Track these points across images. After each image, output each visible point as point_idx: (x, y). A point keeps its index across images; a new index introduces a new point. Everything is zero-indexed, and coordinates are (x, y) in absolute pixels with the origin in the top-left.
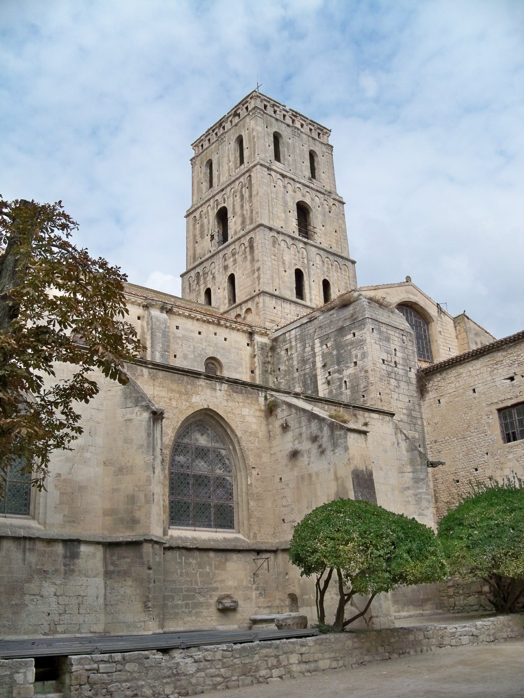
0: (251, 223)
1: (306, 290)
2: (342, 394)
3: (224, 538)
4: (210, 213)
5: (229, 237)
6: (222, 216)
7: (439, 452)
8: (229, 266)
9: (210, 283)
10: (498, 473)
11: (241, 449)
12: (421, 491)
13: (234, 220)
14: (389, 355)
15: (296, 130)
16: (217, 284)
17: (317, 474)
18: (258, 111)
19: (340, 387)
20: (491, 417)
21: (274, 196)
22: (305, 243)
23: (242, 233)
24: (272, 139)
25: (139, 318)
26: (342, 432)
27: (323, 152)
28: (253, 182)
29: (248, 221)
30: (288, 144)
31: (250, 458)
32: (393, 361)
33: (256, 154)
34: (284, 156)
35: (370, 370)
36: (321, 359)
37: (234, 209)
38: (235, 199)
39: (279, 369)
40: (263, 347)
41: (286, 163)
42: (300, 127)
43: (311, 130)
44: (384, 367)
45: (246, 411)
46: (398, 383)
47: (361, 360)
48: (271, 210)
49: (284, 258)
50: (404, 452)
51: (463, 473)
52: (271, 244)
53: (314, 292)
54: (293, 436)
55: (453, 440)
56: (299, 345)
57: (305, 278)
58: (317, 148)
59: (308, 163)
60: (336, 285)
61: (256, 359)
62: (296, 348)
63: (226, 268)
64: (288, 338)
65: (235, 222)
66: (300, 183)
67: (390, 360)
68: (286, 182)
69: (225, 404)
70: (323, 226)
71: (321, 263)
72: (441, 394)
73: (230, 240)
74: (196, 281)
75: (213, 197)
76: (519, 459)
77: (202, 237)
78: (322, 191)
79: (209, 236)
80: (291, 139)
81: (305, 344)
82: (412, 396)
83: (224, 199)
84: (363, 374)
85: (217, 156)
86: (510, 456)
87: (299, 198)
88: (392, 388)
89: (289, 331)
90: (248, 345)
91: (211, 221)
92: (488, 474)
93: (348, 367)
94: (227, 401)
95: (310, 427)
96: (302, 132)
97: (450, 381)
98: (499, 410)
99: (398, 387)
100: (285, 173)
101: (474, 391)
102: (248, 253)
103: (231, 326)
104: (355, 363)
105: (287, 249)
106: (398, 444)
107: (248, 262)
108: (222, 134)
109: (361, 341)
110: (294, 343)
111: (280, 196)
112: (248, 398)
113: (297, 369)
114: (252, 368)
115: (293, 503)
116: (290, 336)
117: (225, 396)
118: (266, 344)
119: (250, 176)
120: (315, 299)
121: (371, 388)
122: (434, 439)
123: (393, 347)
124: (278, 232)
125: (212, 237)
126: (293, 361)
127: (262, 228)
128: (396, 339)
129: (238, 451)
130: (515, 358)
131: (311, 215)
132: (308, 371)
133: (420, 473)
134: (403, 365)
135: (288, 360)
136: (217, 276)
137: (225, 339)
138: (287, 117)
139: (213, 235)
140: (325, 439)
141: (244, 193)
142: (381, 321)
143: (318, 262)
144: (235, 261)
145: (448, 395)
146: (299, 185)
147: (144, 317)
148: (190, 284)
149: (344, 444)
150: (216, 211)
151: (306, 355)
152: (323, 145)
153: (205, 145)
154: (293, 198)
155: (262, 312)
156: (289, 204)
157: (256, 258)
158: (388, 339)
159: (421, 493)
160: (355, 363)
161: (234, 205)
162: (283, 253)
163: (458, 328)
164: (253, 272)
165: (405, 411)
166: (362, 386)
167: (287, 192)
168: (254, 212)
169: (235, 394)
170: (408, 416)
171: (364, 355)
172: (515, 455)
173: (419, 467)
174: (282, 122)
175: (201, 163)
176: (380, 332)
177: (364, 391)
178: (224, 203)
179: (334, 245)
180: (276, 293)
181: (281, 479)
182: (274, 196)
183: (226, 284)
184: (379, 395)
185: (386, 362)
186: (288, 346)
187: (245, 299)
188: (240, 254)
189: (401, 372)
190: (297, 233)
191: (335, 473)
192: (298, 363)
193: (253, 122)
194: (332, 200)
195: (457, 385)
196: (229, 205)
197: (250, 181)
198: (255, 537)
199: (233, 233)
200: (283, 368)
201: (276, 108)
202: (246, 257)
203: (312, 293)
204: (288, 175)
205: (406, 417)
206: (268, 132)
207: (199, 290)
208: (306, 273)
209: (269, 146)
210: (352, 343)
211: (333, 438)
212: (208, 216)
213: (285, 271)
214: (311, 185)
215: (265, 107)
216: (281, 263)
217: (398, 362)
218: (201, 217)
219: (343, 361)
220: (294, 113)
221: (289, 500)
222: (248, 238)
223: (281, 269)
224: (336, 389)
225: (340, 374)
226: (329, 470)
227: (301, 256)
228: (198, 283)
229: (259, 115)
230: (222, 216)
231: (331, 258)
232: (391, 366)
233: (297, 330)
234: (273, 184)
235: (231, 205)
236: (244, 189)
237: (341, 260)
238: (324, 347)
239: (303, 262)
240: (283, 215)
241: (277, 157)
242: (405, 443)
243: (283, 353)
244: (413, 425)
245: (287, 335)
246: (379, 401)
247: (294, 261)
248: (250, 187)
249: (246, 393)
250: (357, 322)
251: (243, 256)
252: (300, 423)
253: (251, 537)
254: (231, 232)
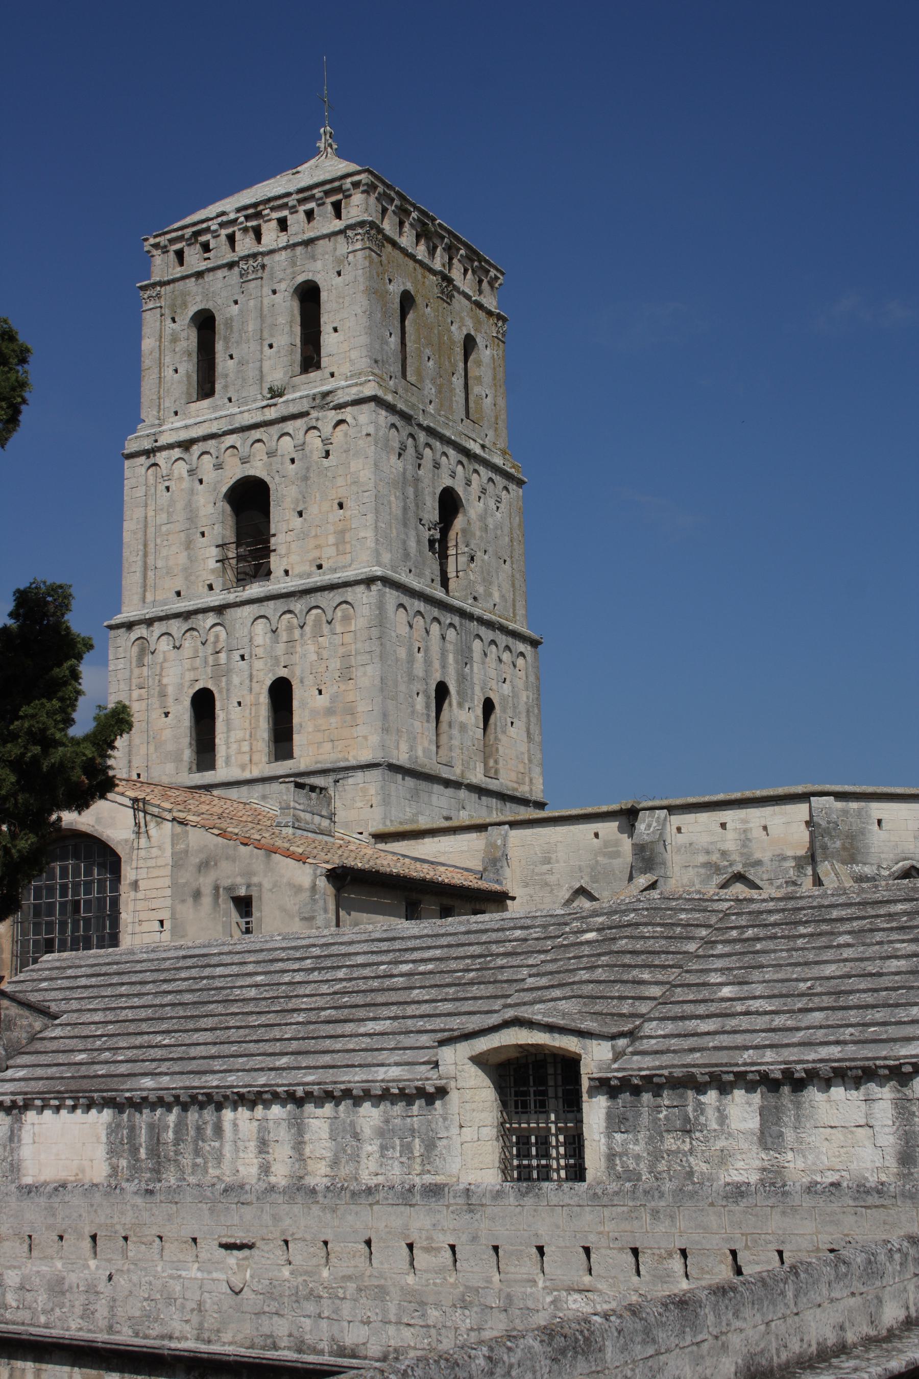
15: (251, 262)
21: (163, 517)
49: (165, 681)
58: (319, 265)
87: (234, 472)
111: (180, 505)
156: (202, 512)
162: (162, 669)
167: (201, 481)
179: (328, 555)
201: (203, 239)
208: (220, 692)
213: (167, 714)
216: (155, 702)
223: (157, 714)
231: (298, 606)
239: (217, 665)
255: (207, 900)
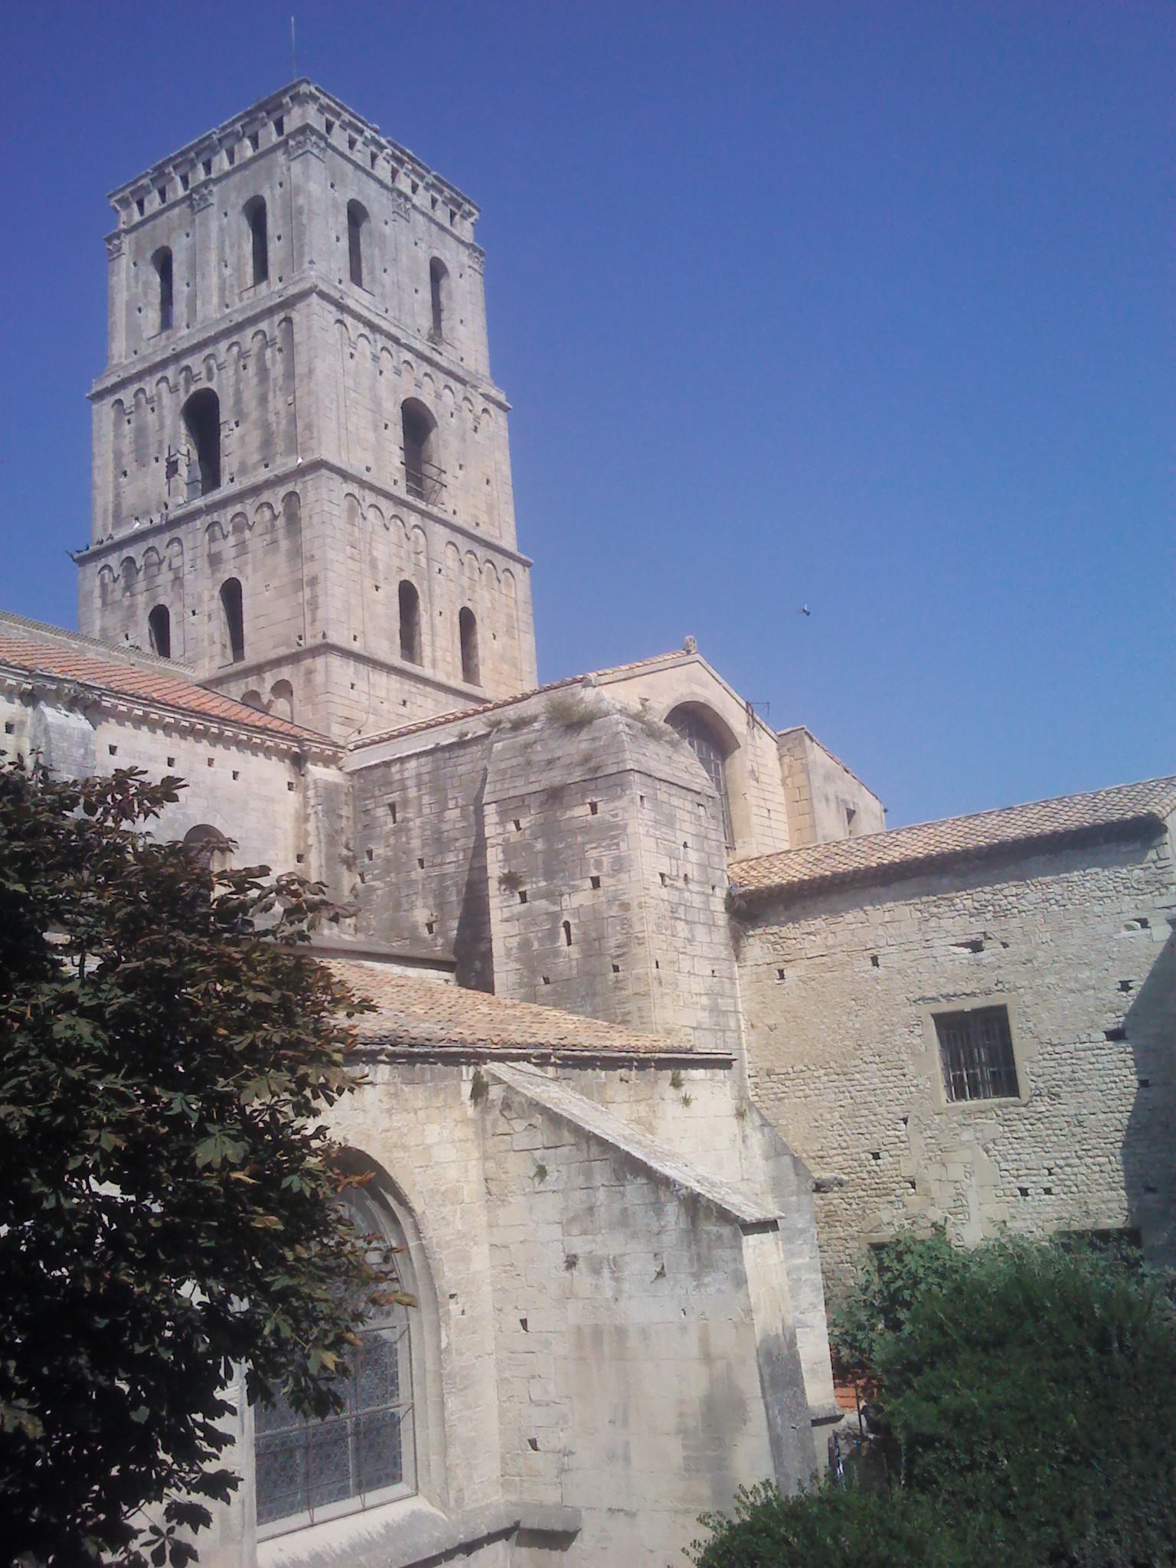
0: (293, 447)
1: (425, 638)
2: (556, 953)
3: (387, 1526)
4: (167, 399)
5: (225, 479)
6: (203, 416)
7: (779, 1100)
8: (225, 556)
9: (165, 593)
10: (935, 1171)
11: (422, 1248)
12: (799, 1261)
13: (237, 430)
14: (674, 862)
16: (189, 601)
17: (644, 1334)
18: (314, 138)
19: (552, 935)
20: (918, 1031)
21: (350, 383)
22: (423, 514)
23: (263, 475)
24: (344, 219)
25: (9, 728)
26: (726, 1231)
27: (462, 266)
28: (297, 338)
29: (280, 445)
30: (382, 235)
31: (446, 1269)
32: (682, 875)
33: (307, 259)
34: (371, 272)
35: (634, 904)
36: (501, 856)
37: (238, 401)
38: (243, 373)
39: (370, 853)
40: (329, 794)
41: (377, 291)
42: (408, 191)
43: (434, 201)
44: (664, 893)
45: (433, 1133)
46: (691, 931)
47: (613, 876)
48: (343, 421)
49: (375, 553)
50: (759, 1160)
51: (840, 1158)
52: (345, 515)
53: (441, 642)
54: (566, 1209)
55: (816, 1074)
56: (426, 799)
57: (422, 605)
59: (426, 294)
60: (487, 621)
61: (311, 826)
62: (420, 806)
63: (215, 560)
64: (397, 777)
65: (242, 438)
66: (410, 349)
67: (674, 873)
68: (379, 347)
69: (385, 1123)
70: (461, 467)
71: (455, 565)
72: (789, 957)
73: (226, 489)
74: (122, 581)
75: (177, 357)
76: (991, 1146)
77: (141, 461)
78: (461, 373)
79: (163, 464)
80: (390, 223)
81: (446, 798)
82: (717, 959)
83: (209, 370)
84: (614, 911)
85: (185, 240)
86: (967, 1135)
88: (679, 943)
89: (402, 760)
90: (290, 786)
91: (168, 422)
92: (907, 1169)
93: (575, 889)
94: (389, 1111)
95: (623, 1195)
96: (414, 206)
97: (813, 929)
98: (940, 1019)
99: (690, 941)
100: (377, 320)
101: (875, 961)
102: (281, 533)
103: (250, 739)
104: (596, 882)
105: (381, 531)
106: (744, 1139)
107: (281, 559)
108: (205, 184)
109: (616, 827)
110: (412, 793)
112: (437, 1092)
113: (421, 861)
114: (298, 847)
115: (566, 1401)
116: (401, 771)
117: (385, 1099)
118: (336, 784)
119: (288, 320)
120: (444, 660)
121: (637, 950)
122: (766, 1065)
123: (681, 838)
124: (363, 484)
125: (172, 468)
126: (409, 838)
127: (324, 471)
128: (687, 817)
129: (413, 1253)
130: (988, 897)
131: (432, 436)
132: (450, 869)
133: (796, 1215)
134: (700, 883)
135: (395, 833)
136: (189, 578)
137: (235, 775)
138: (380, 161)
139: (176, 462)
140: (670, 1238)
141: (269, 363)
142: (659, 775)
143: (450, 563)
144: (242, 547)
145: (807, 962)
146: (408, 356)
147: (23, 723)
148: (103, 586)
149: (732, 1266)
150: (183, 398)
151: (445, 827)
152: (462, 248)
153: (151, 203)
154: (395, 390)
155: (322, 698)
157: (305, 548)
158: (670, 822)
159: (798, 1268)
160: (596, 882)
161: (238, 393)
163: (786, 760)
164: (298, 585)
165: (705, 1000)
166: (612, 942)
167: (381, 372)
168: (300, 424)
169: (406, 1089)
170: (711, 1011)
171: (620, 866)
172: (979, 1135)
173: (794, 1198)
174: (369, 174)
175: (138, 251)
176: (657, 804)
177: (619, 956)
178: (210, 379)
179: (484, 518)
180: (356, 647)
181: (524, 1322)
182: (350, 383)
183: (214, 604)
184: (655, 970)
185: (668, 881)
186: (395, 797)
187: (273, 655)
188: (258, 529)
189: (697, 901)
190: (402, 484)
191: (704, 1340)
192: (424, 846)
193: (297, 167)
194: (481, 398)
195: (830, 942)
196: (223, 385)
197: (289, 334)
198: (459, 1501)
199: (235, 468)
200: (379, 850)
202: (274, 542)
203: (438, 644)
204: (384, 325)
205: (706, 1014)
206: (334, 199)
207: (132, 606)
209: (338, 239)
210: (586, 829)
211: (697, 1241)
212: (161, 407)
213: (377, 588)
214: (437, 357)
215: (329, 126)
216: (366, 567)
217: (690, 876)
218: (138, 405)
219: (563, 871)
220: (398, 153)
221: (551, 1388)
222: (282, 491)
223: (369, 583)
224: (539, 940)
225: (554, 903)
226: (683, 1329)
227: (411, 549)
228: (128, 587)
229: (315, 151)
230: (203, 416)
231: (481, 552)
232: (677, 889)
233: (423, 760)
234: (348, 350)
235: (231, 390)
236: (268, 352)
237: (500, 557)
238: (512, 827)
240: (371, 436)
241: (356, 277)
242: (760, 1136)
243: (382, 812)
244: (720, 1034)
245: (395, 769)
246: (656, 984)
247: (396, 562)
248: (289, 349)
249: (433, 1079)
250: (601, 779)
251: (268, 537)
252: (588, 1175)
253: (452, 1503)
254: (228, 464)
255: (833, 805)
